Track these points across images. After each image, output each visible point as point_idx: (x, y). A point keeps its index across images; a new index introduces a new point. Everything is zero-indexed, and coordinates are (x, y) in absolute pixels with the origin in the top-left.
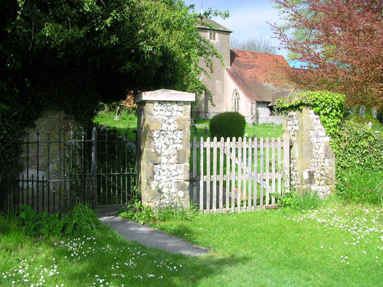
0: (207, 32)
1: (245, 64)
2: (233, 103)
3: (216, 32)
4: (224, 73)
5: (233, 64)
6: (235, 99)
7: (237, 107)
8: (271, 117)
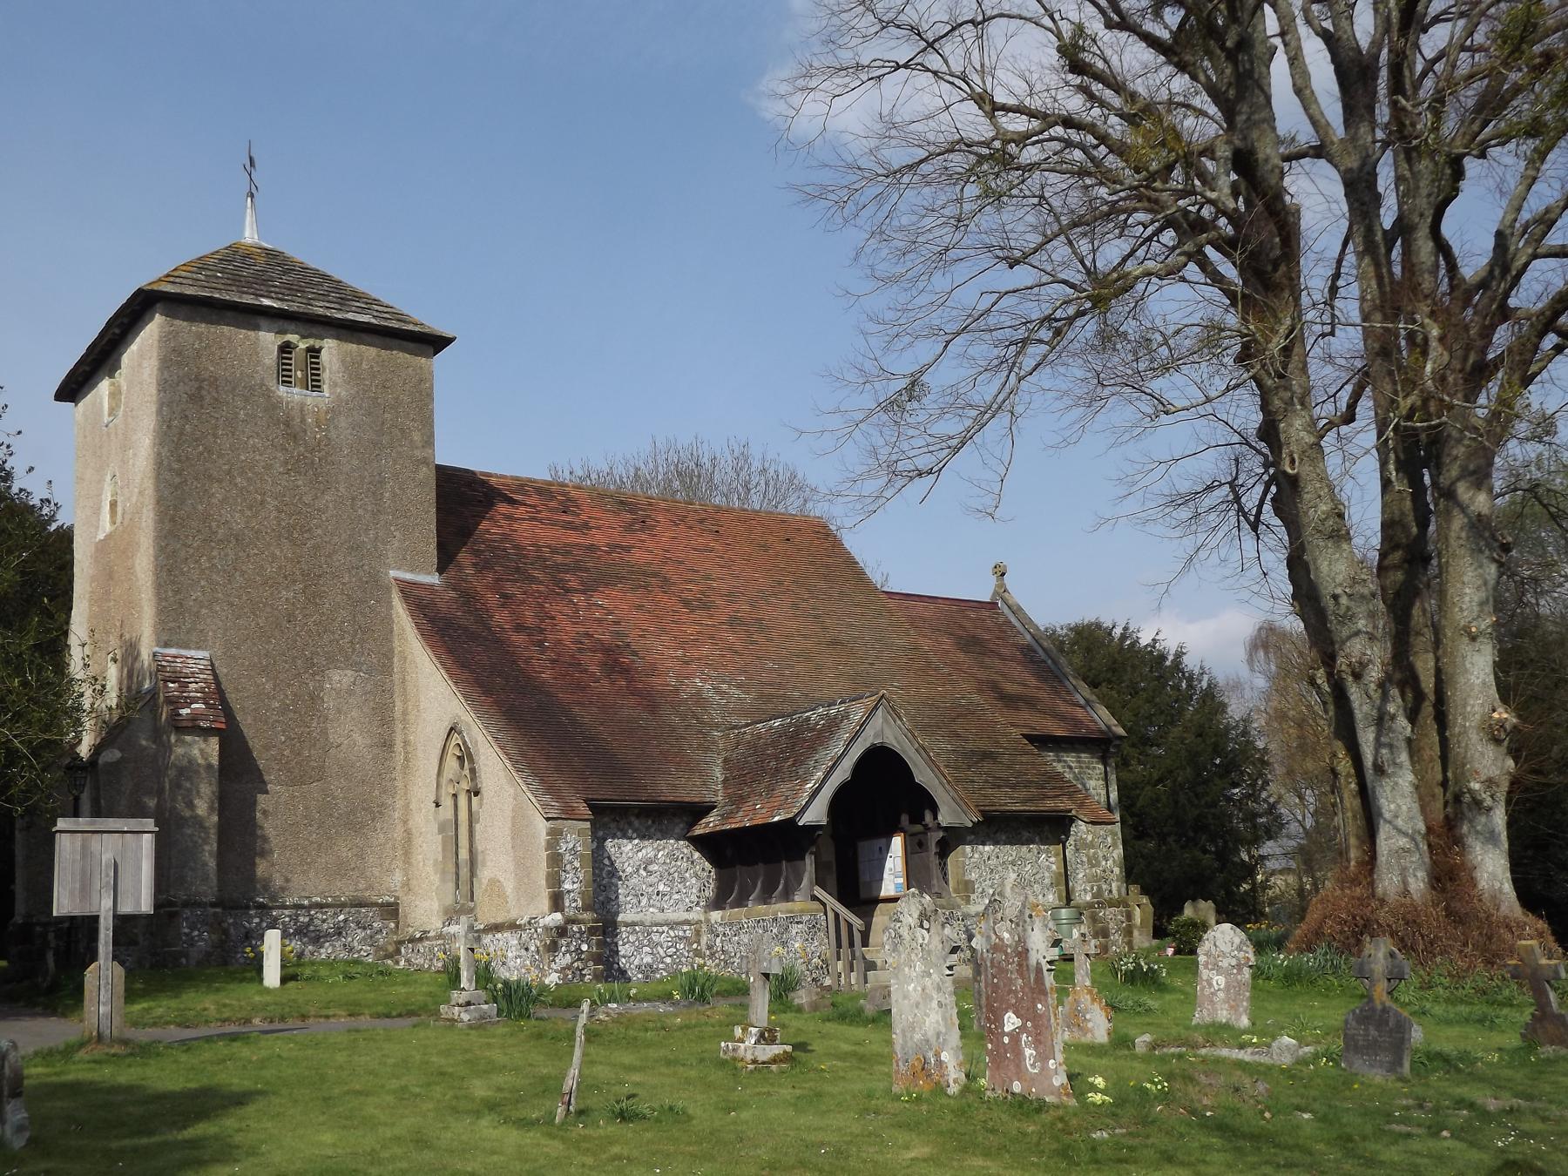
0: (257, 328)
1: (559, 559)
2: (442, 829)
4: (388, 621)
5: (464, 557)
7: (464, 854)
8: (716, 916)
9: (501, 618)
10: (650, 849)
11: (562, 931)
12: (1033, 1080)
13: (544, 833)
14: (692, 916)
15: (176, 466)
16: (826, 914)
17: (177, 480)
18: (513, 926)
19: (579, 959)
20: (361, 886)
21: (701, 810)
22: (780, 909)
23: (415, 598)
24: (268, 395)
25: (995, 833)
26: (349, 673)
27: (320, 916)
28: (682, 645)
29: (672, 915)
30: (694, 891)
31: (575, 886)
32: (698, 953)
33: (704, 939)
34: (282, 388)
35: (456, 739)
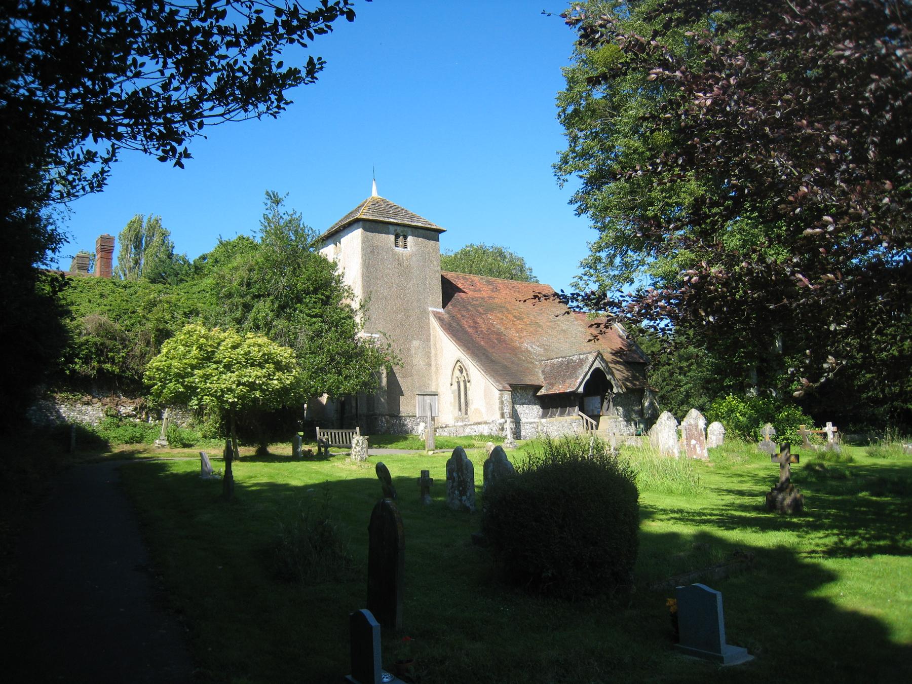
2: (453, 392)
3: (409, 230)
4: (428, 324)
6: (458, 383)
7: (463, 400)
8: (544, 420)
9: (464, 323)
12: (699, 455)
18: (486, 423)
21: (540, 387)
28: (517, 332)
32: (537, 432)
35: (459, 364)
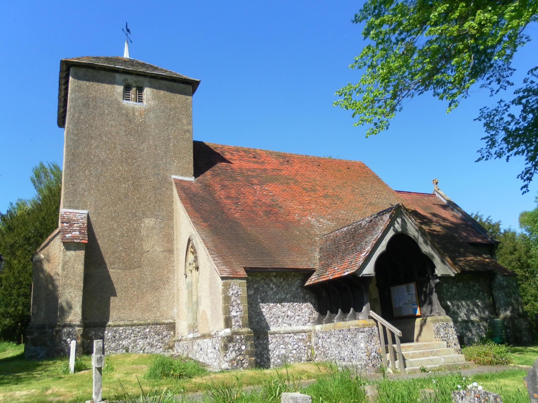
1: (250, 173)
3: (146, 81)
8: (318, 327)
10: (282, 293)
11: (230, 339)
13: (221, 286)
14: (306, 328)
15: (75, 132)
16: (377, 326)
17: (76, 138)
18: (210, 336)
19: (240, 354)
20: (158, 315)
21: (309, 273)
22: (351, 324)
23: (181, 186)
24: (119, 103)
25: (457, 282)
26: (153, 219)
27: (137, 330)
29: (295, 328)
30: (307, 315)
31: (238, 313)
32: (310, 347)
33: (313, 340)
34: (125, 101)
